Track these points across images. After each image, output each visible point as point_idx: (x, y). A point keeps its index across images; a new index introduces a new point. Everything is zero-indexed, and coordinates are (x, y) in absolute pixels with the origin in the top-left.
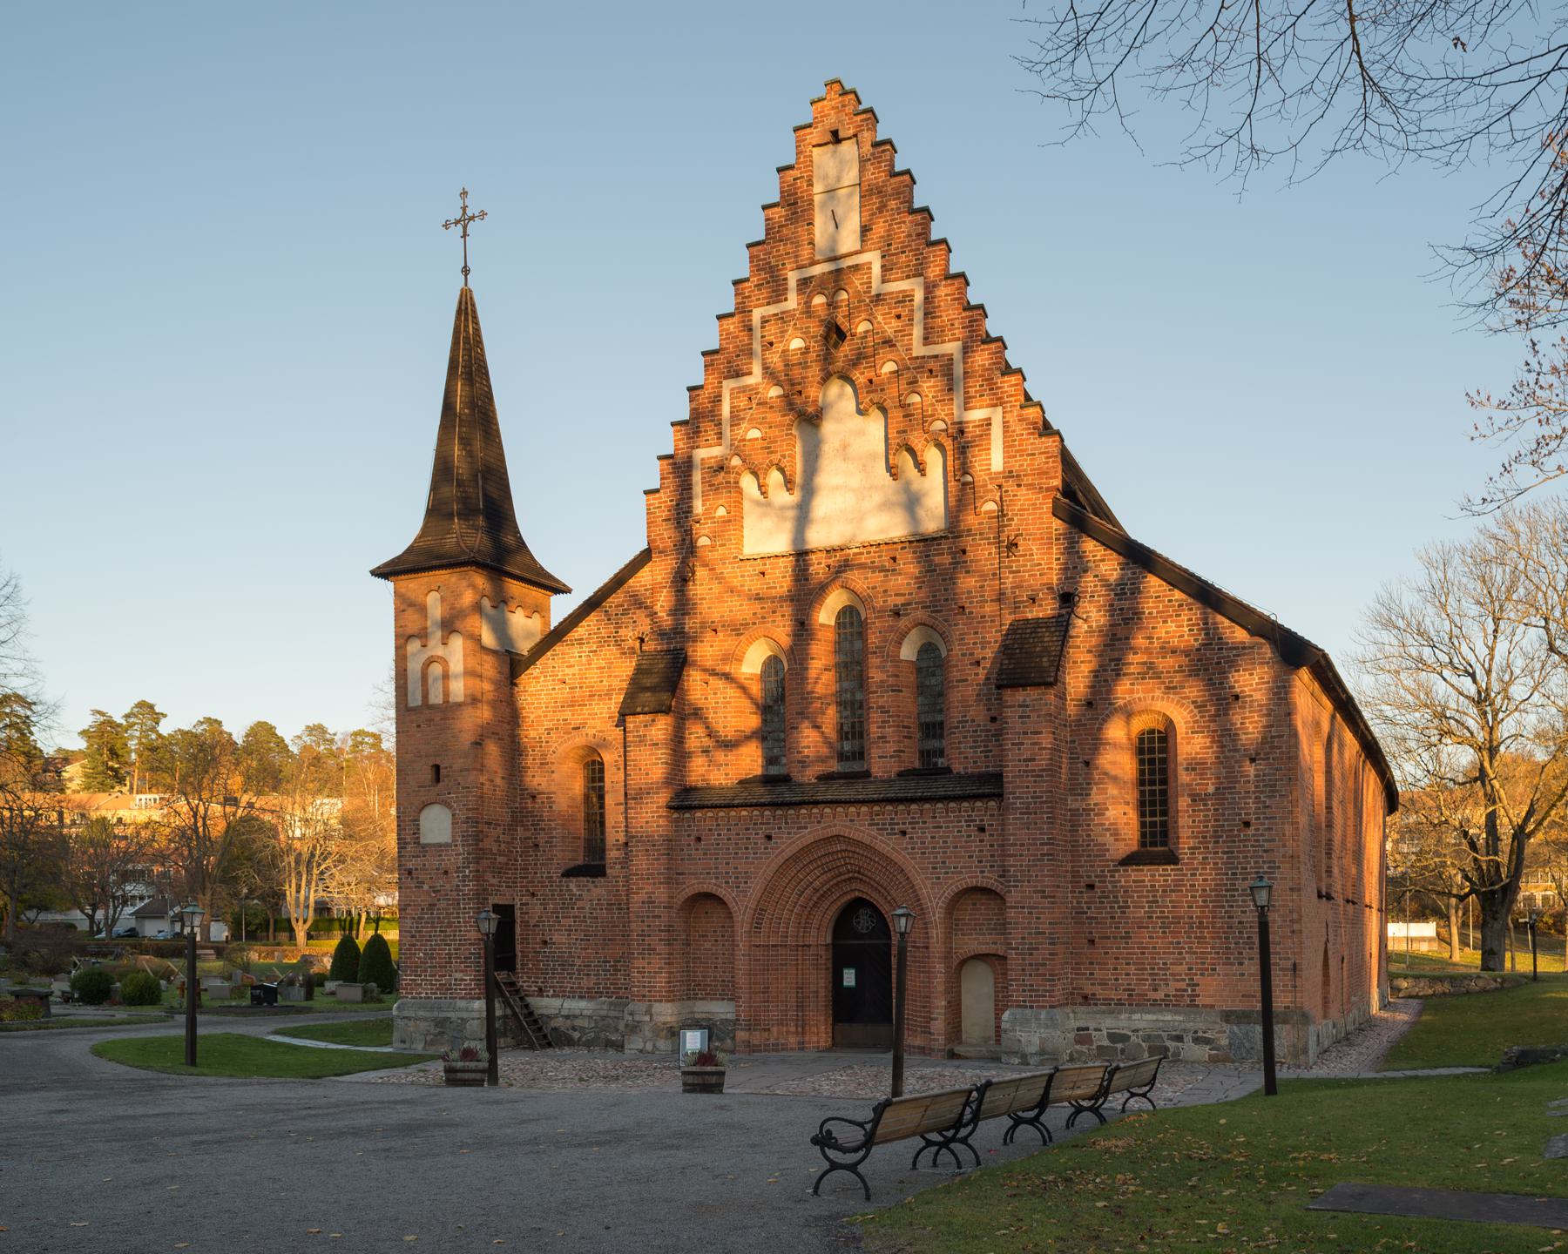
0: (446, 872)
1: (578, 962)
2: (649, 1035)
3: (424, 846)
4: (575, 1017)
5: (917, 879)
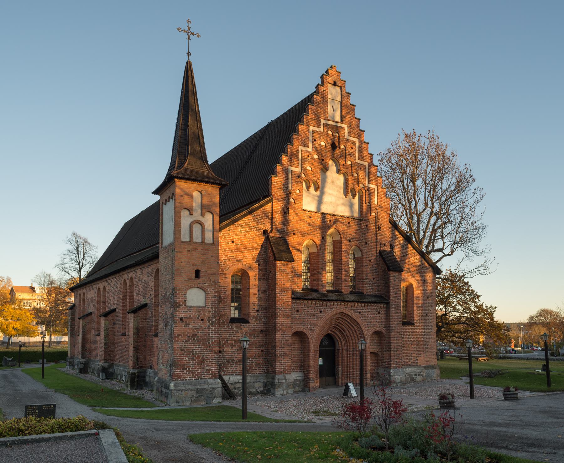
0: (202, 320)
1: (236, 359)
2: (285, 387)
3: (190, 307)
4: (236, 383)
5: (363, 328)
